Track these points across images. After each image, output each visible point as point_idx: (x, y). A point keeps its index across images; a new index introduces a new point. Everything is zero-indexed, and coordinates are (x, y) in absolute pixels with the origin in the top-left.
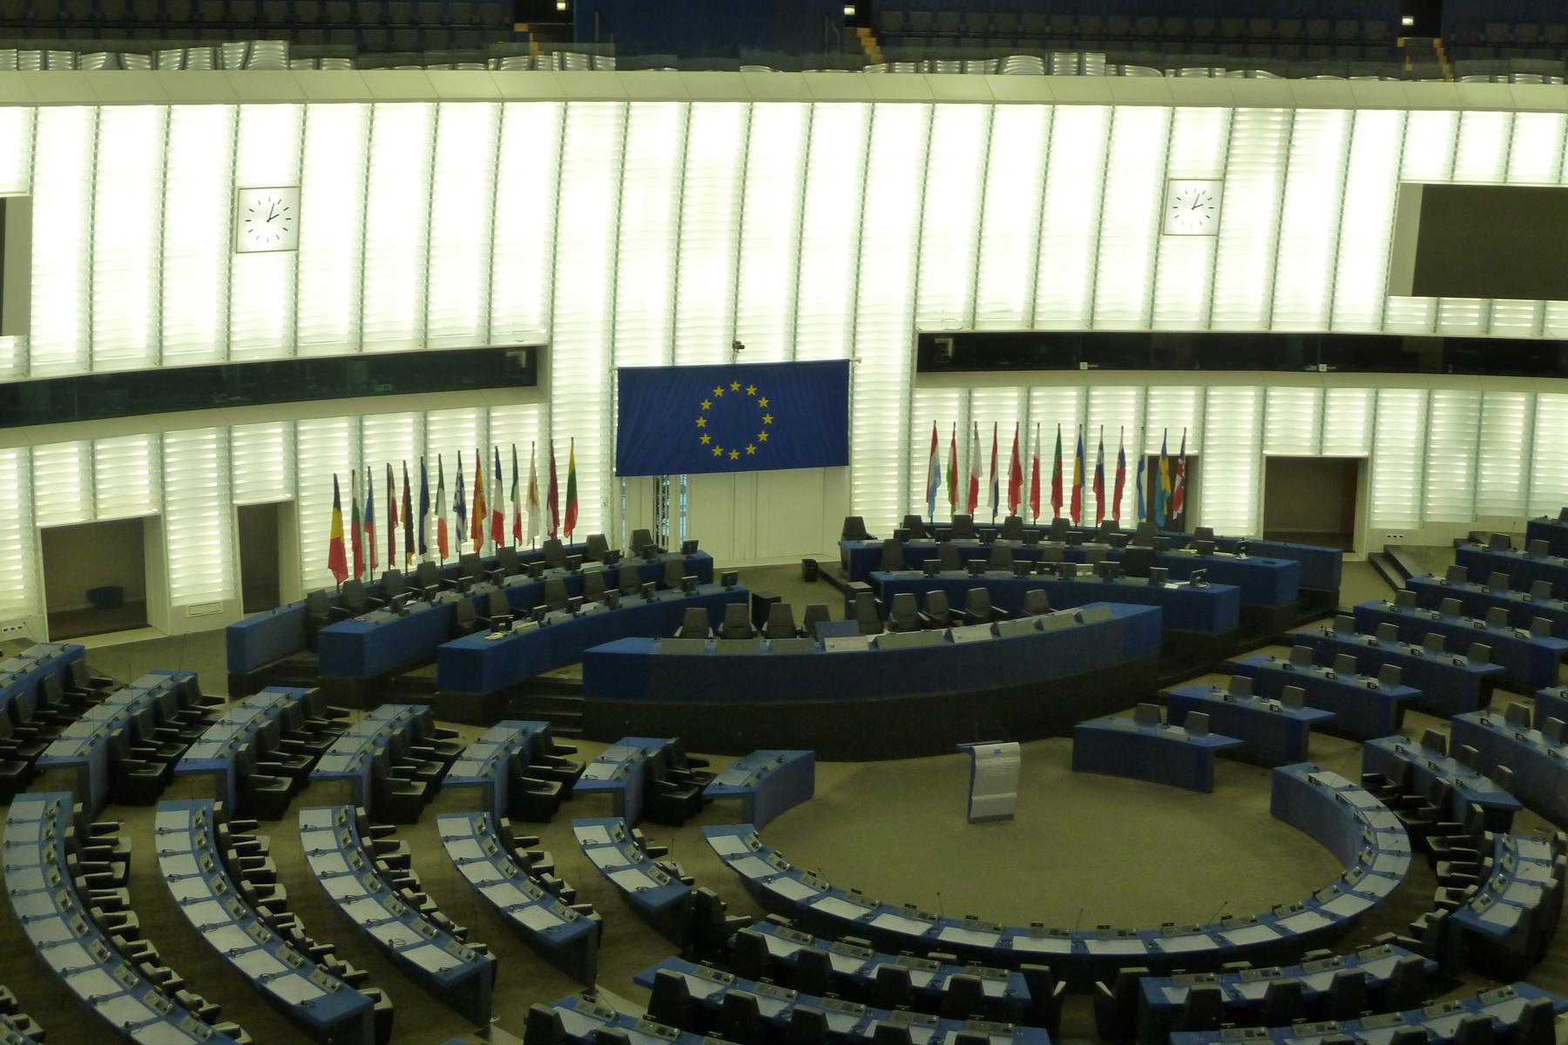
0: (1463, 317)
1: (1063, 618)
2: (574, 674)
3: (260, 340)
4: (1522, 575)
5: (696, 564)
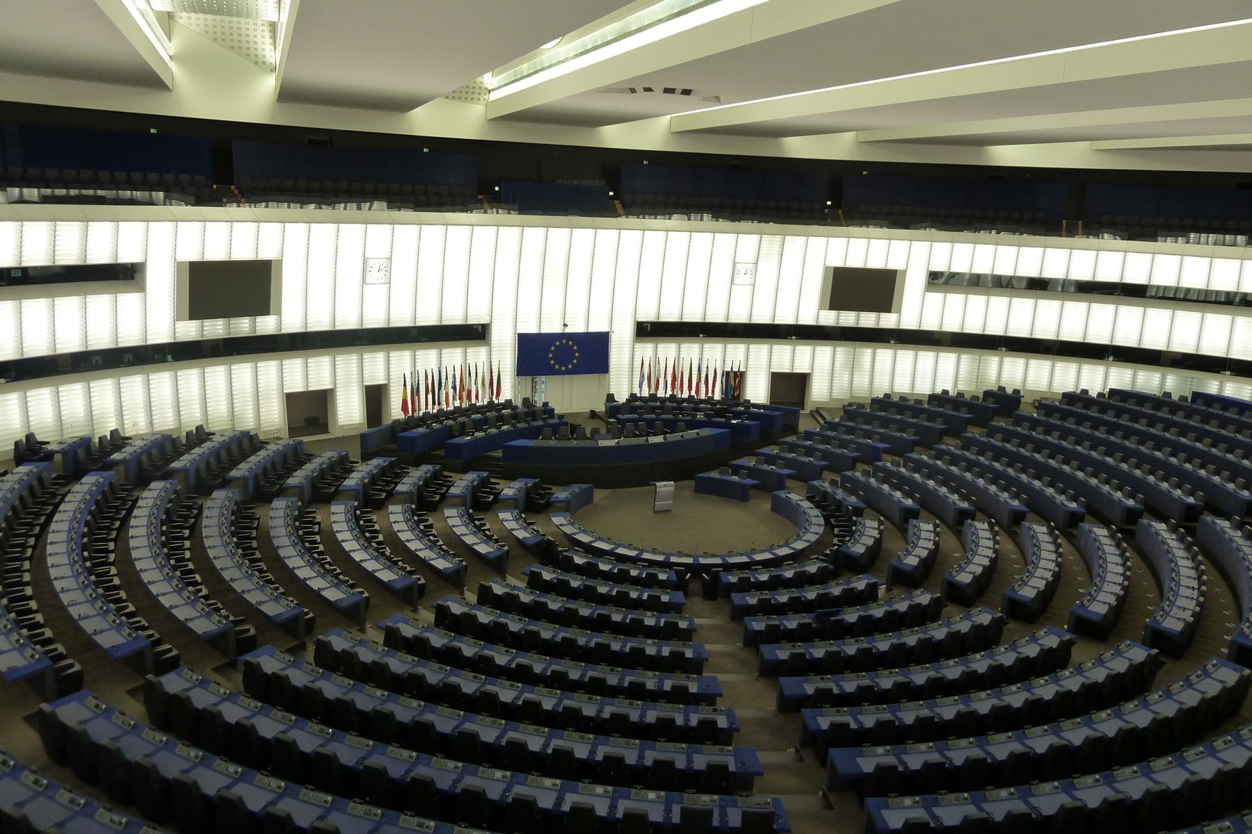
0: (848, 319)
1: (692, 433)
2: (499, 454)
3: (375, 320)
4: (869, 419)
5: (548, 410)
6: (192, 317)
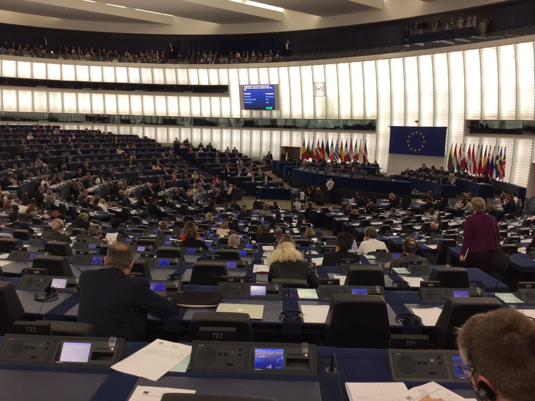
6: (246, 108)
